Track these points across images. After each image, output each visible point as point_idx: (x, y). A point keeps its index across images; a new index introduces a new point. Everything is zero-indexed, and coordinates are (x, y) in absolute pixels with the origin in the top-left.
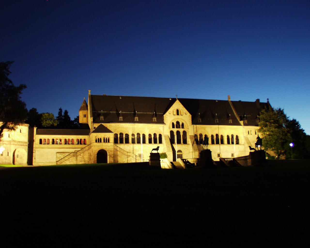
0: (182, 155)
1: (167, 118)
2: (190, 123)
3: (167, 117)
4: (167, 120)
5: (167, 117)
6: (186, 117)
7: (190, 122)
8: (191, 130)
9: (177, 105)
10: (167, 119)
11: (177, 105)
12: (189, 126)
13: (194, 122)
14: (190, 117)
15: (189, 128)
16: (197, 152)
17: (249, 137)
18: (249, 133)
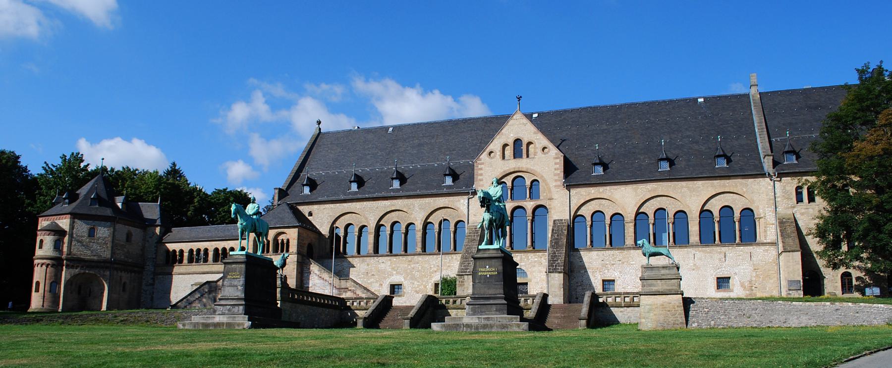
0: (526, 284)
1: (480, 172)
2: (556, 181)
3: (481, 169)
4: (480, 177)
5: (481, 169)
6: (545, 164)
7: (557, 178)
8: (560, 203)
9: (519, 127)
10: (481, 175)
11: (519, 127)
12: (553, 190)
13: (572, 173)
14: (558, 161)
15: (555, 196)
16: (557, 275)
17: (802, 214)
18: (799, 199)
